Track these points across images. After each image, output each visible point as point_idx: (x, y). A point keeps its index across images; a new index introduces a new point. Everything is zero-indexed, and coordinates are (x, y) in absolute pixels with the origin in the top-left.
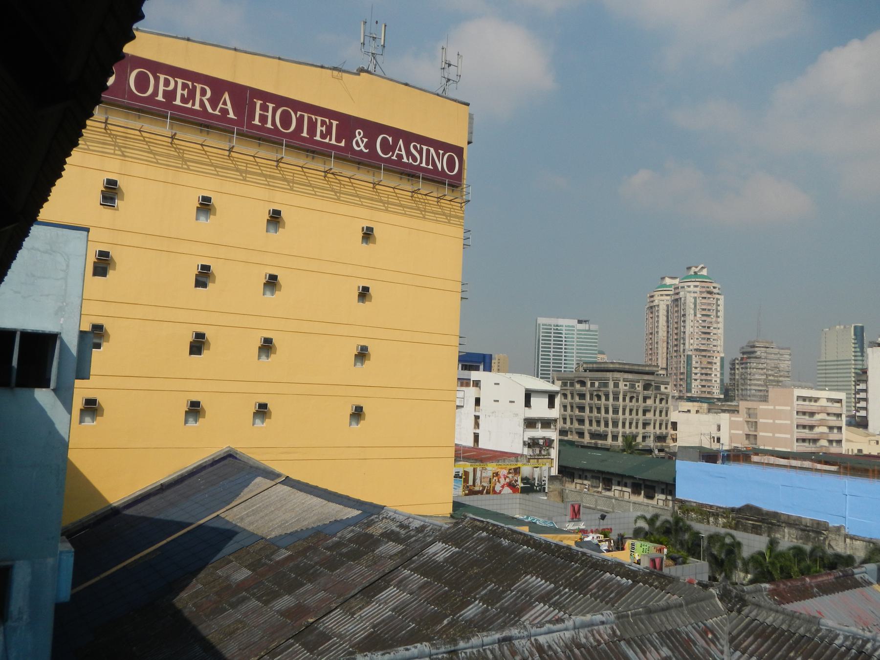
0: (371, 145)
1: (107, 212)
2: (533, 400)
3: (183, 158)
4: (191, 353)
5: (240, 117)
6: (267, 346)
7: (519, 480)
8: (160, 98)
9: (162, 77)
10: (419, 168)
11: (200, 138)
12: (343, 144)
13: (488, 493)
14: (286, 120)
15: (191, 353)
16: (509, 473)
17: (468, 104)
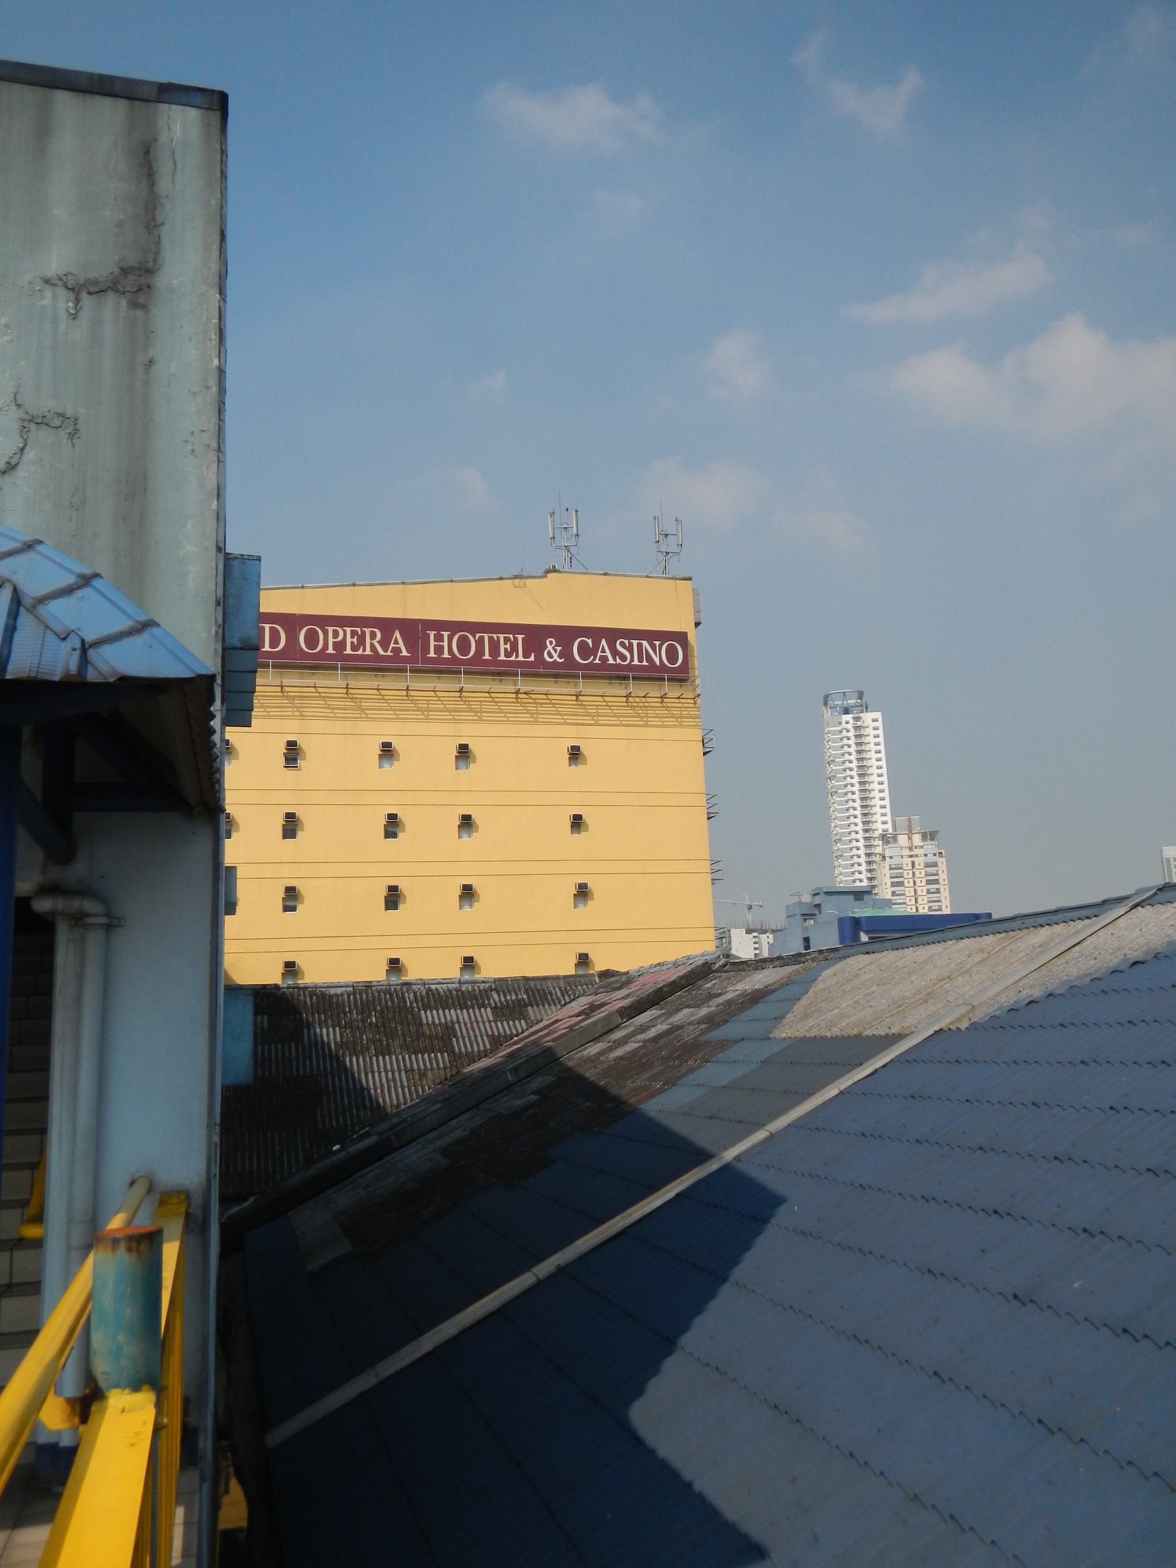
0: (566, 653)
1: (291, 773)
3: (360, 708)
4: (387, 908)
5: (415, 651)
6: (468, 893)
8: (331, 650)
9: (330, 629)
10: (630, 667)
11: (374, 684)
12: (532, 658)
14: (464, 646)
15: (387, 908)
17: (690, 579)
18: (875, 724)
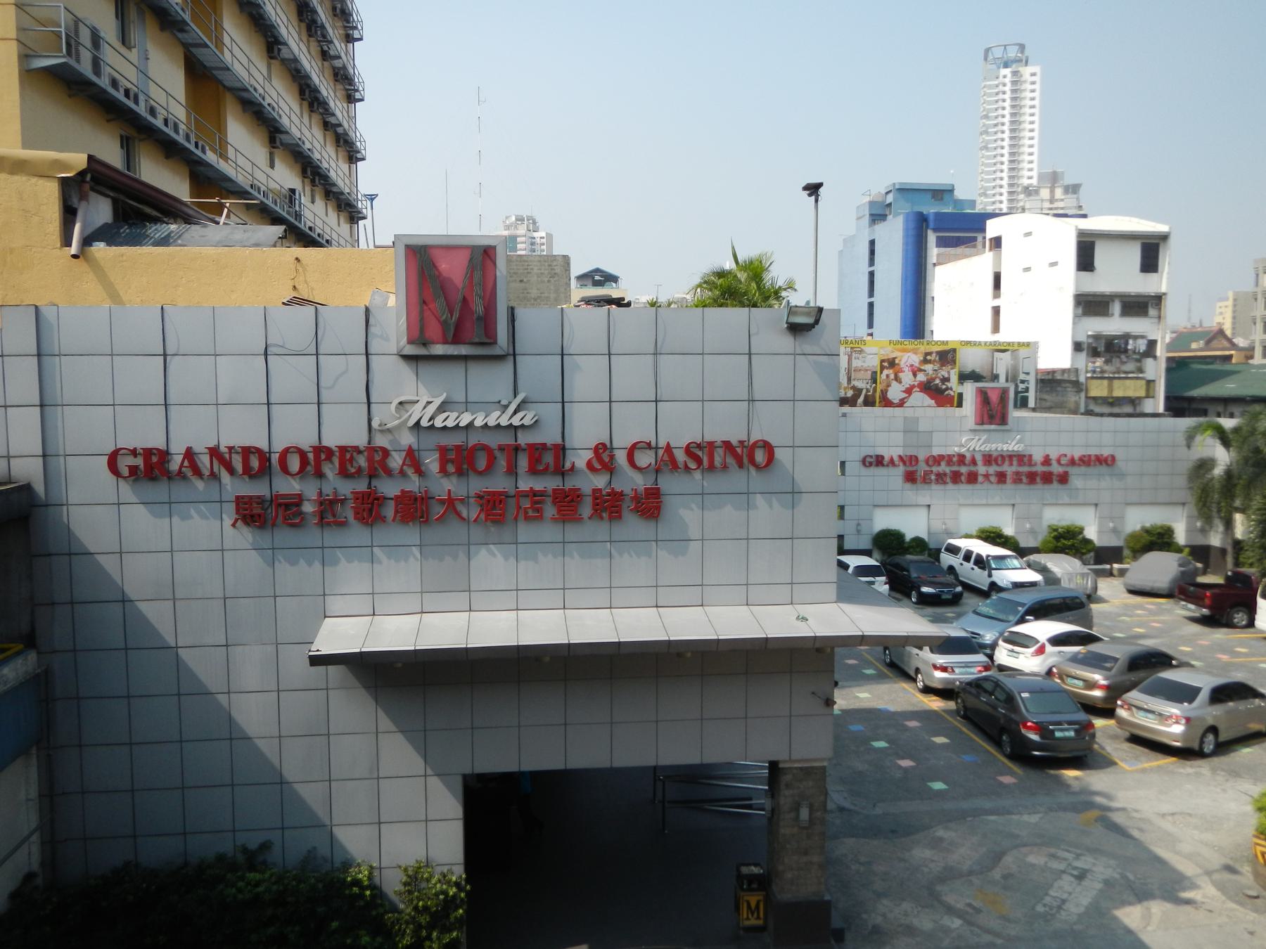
2: (1101, 254)
13: (869, 402)
16: (925, 361)
18: (1033, 79)
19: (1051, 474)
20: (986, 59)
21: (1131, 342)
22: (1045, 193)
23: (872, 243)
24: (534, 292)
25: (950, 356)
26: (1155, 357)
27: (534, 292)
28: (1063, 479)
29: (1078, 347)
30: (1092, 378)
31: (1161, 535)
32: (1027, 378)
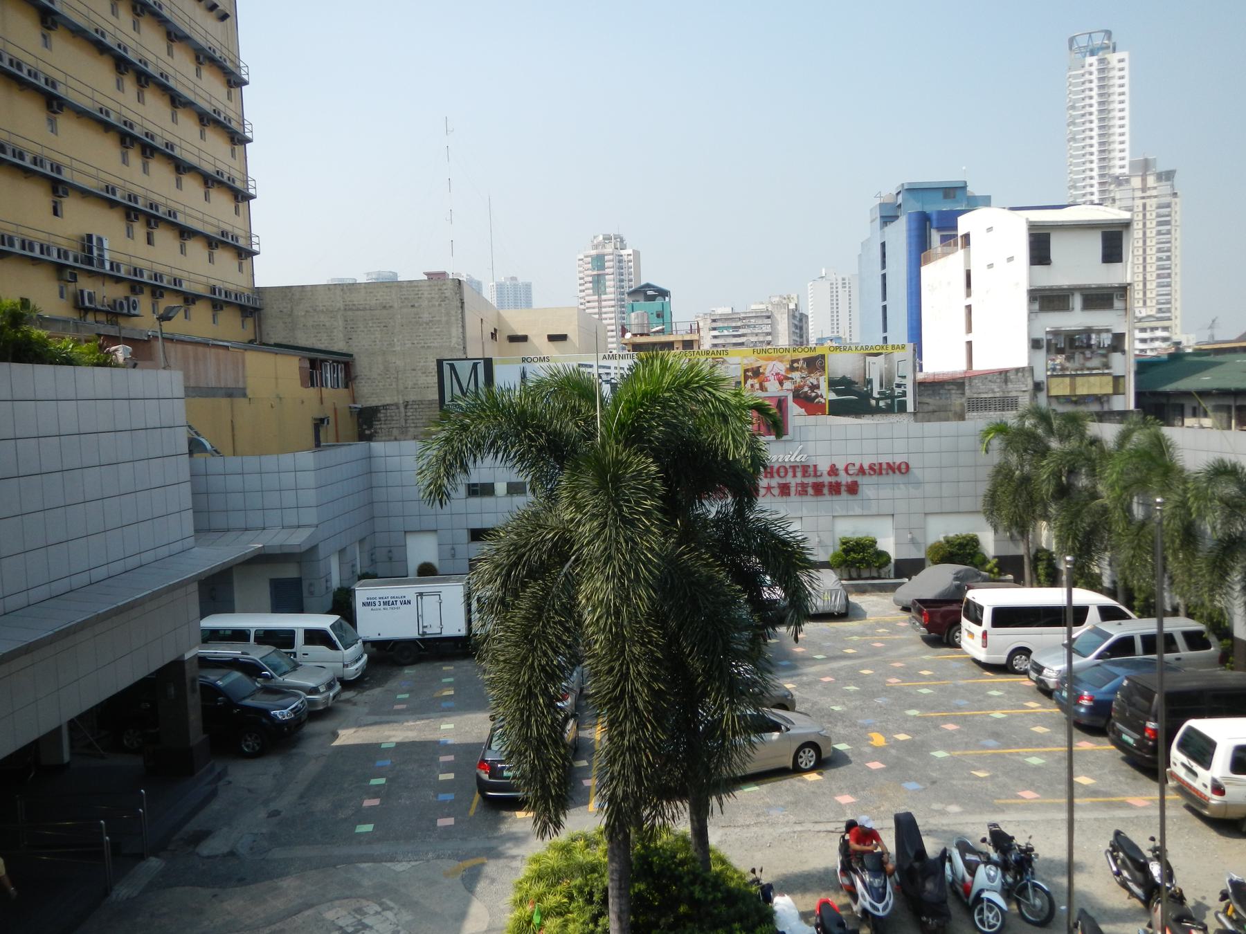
2: (1058, 246)
7: (824, 385)
16: (792, 369)
18: (1121, 65)
19: (838, 485)
20: (1071, 48)
21: (1093, 336)
22: (1136, 182)
23: (883, 245)
24: (426, 317)
25: (818, 363)
26: (1123, 352)
27: (426, 317)
28: (853, 489)
29: (1035, 344)
30: (1052, 376)
31: (962, 546)
32: (904, 381)
